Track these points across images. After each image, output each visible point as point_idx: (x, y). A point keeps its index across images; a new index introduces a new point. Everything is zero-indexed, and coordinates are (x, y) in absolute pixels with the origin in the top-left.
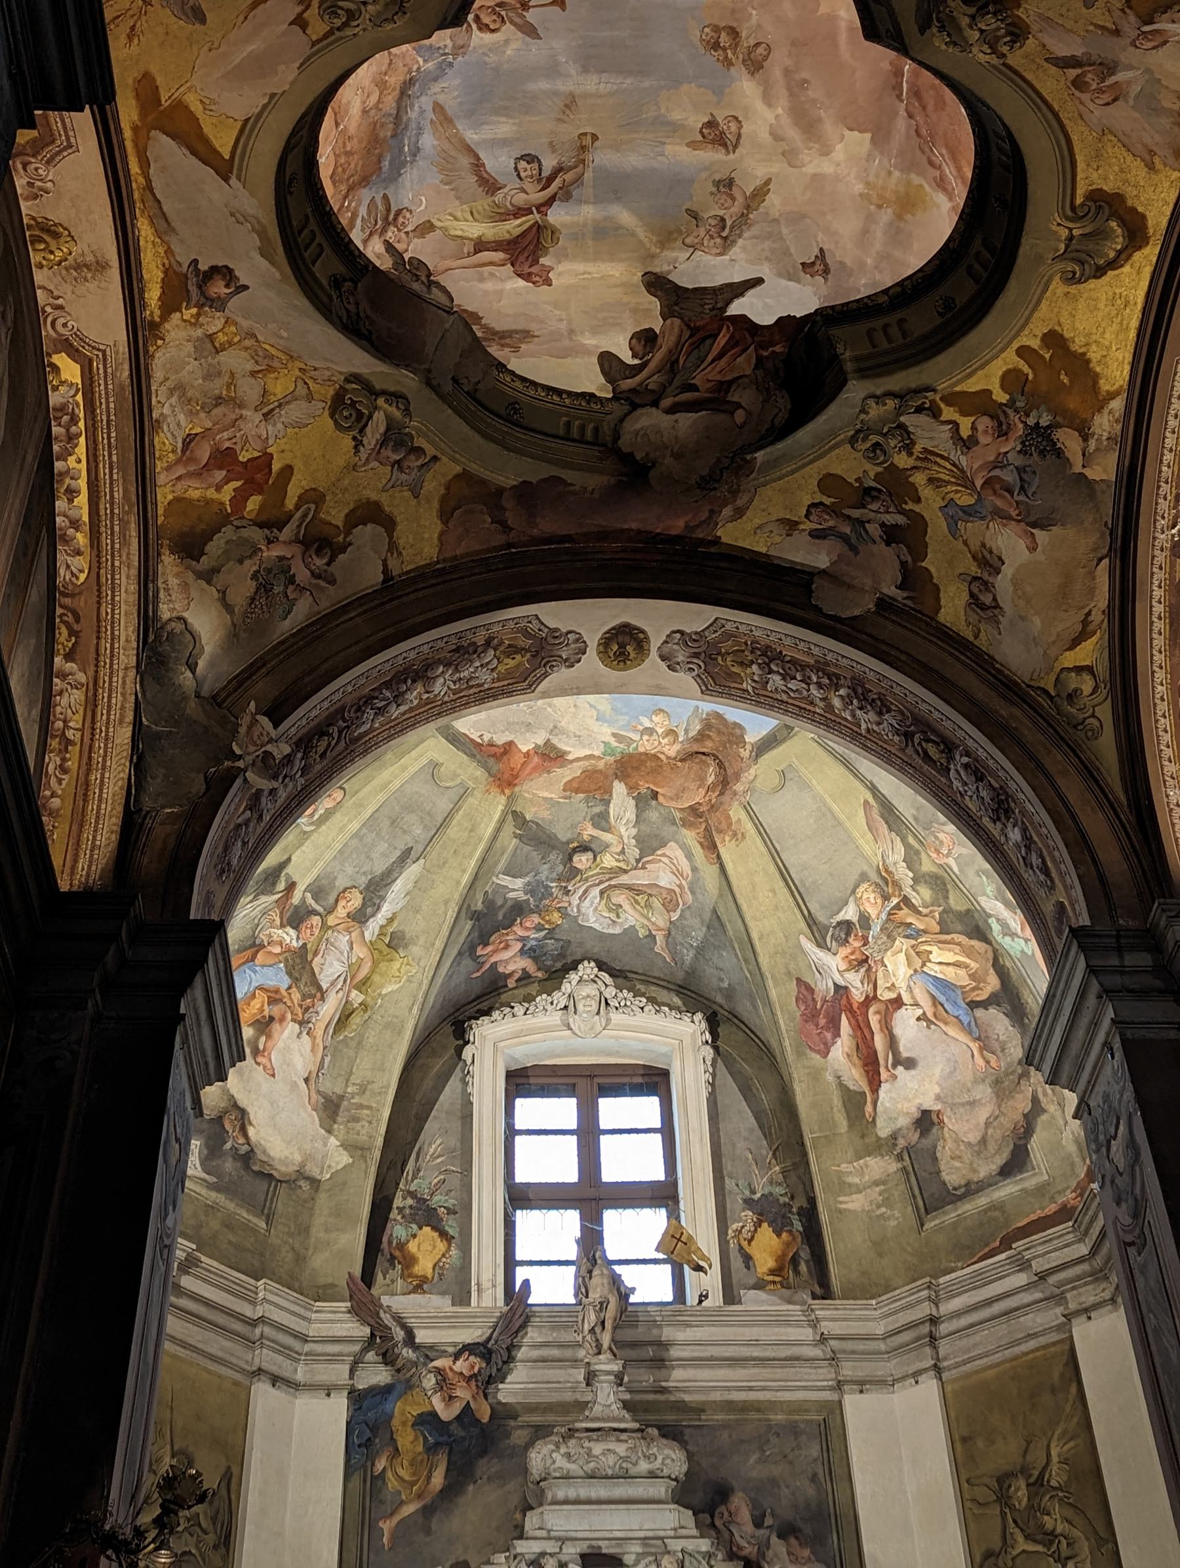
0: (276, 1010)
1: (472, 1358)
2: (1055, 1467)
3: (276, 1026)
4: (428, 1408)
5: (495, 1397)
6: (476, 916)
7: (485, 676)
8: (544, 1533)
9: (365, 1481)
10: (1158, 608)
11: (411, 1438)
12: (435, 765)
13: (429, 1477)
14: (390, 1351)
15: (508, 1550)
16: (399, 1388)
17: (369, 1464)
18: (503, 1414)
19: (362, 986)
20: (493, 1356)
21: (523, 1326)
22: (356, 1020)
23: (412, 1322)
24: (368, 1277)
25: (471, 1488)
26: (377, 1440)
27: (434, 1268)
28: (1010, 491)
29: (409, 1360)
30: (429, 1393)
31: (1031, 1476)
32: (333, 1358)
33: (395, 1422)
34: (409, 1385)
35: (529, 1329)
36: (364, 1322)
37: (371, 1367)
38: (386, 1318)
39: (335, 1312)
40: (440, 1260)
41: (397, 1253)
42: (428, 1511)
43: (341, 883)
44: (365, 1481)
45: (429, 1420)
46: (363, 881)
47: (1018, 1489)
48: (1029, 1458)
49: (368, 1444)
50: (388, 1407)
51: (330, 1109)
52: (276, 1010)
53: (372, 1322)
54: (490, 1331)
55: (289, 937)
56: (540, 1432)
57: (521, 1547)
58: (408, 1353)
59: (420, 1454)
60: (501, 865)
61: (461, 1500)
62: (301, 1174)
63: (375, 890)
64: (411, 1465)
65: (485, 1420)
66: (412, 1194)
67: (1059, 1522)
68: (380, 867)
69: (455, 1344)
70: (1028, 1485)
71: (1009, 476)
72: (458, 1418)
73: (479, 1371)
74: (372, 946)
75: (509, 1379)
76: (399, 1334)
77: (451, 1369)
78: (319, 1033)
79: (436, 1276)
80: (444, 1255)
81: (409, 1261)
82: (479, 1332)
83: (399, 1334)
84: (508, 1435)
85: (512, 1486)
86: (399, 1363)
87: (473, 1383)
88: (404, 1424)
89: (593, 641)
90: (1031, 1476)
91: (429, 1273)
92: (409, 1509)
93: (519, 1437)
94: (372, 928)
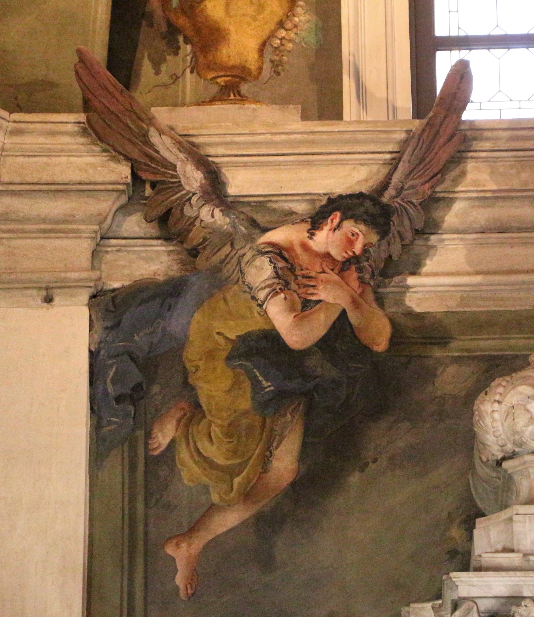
1: (349, 226)
4: (255, 325)
5: (400, 302)
8: (514, 559)
9: (133, 467)
11: (226, 383)
13: (266, 459)
14: (176, 212)
15: (439, 596)
16: (197, 283)
17: (140, 433)
18: (420, 335)
20: (391, 219)
21: (457, 159)
23: (216, 152)
24: (122, 61)
25: (355, 479)
26: (156, 389)
27: (261, 50)
29: (215, 231)
30: (261, 295)
32: (55, 228)
33: (192, 354)
34: (219, 281)
35: (470, 165)
36: (117, 153)
37: (138, 247)
38: (165, 147)
39: (53, 134)
40: (272, 35)
41: (182, 21)
44: (133, 467)
45: (263, 347)
49: (135, 396)
50: (175, 323)
53: (135, 154)
54: (384, 171)
56: (498, 367)
57: (466, 584)
58: (212, 217)
59: (245, 413)
61: (338, 502)
64: (229, 434)
65: (381, 344)
69: (310, 197)
72: (325, 344)
73: (365, 250)
75: (429, 265)
76: (193, 178)
77: (305, 247)
79: (267, 66)
80: (281, 24)
81: (208, 38)
82: (362, 173)
83: (193, 178)
84: (429, 375)
85: (442, 473)
86: (196, 236)
87: (353, 275)
88: (210, 355)
91: (251, 59)
92: (229, 520)
93: (450, 379)
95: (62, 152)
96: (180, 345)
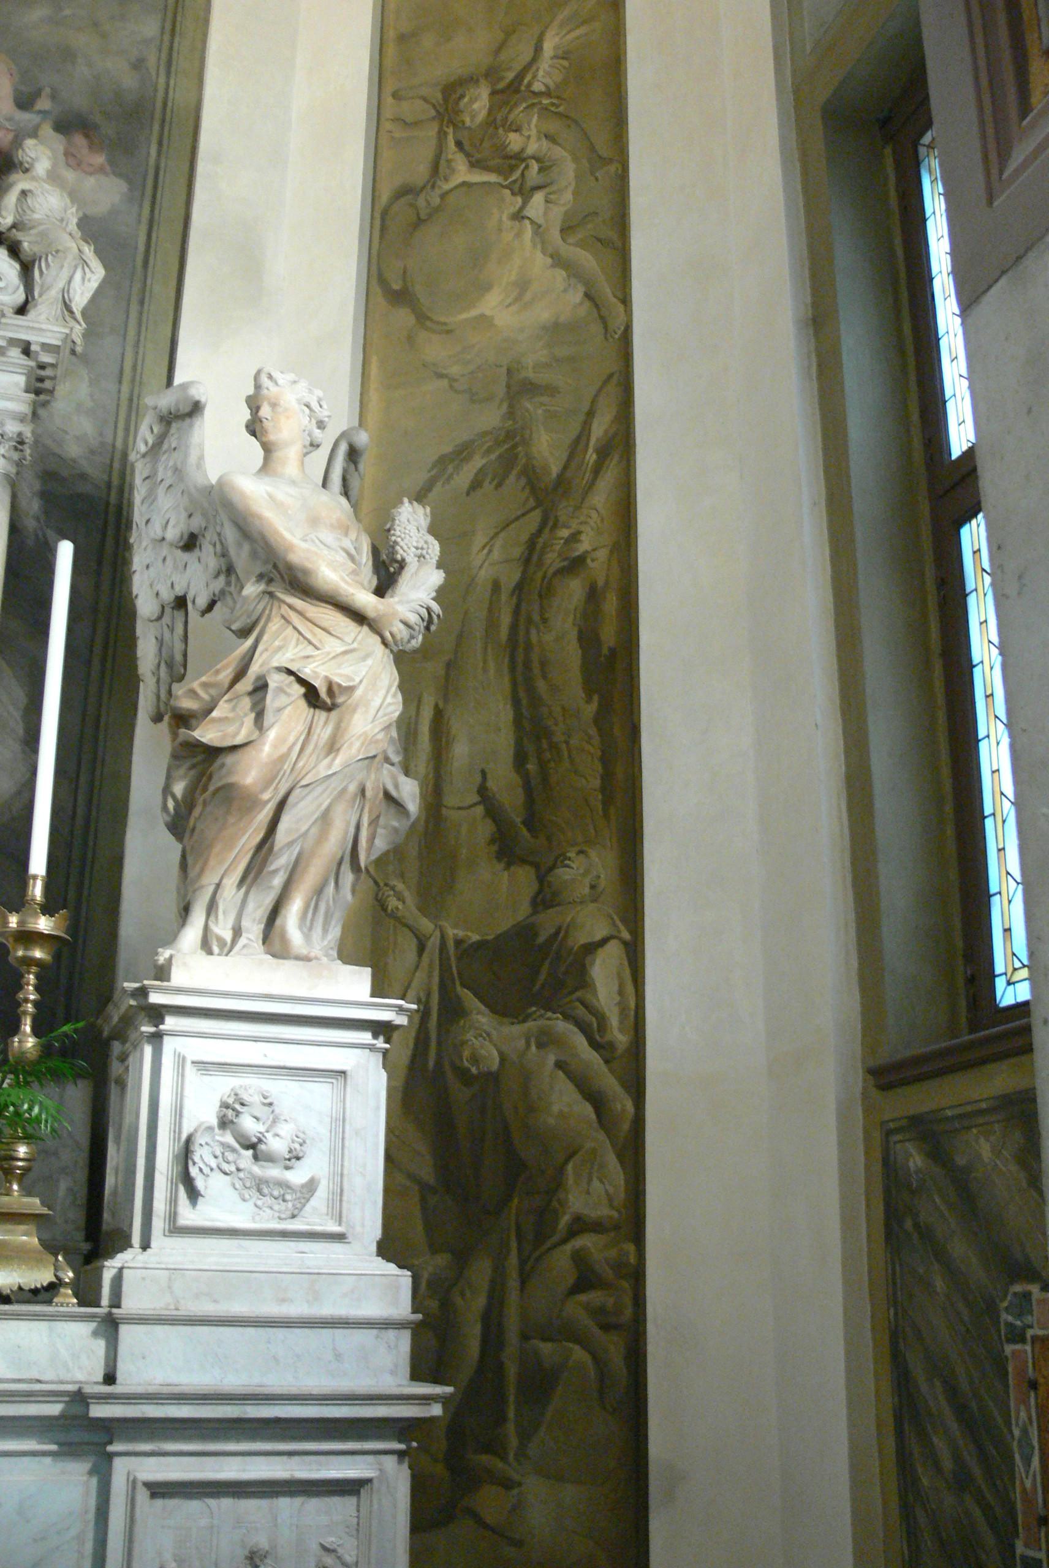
2: (545, 65)
31: (502, 78)
47: (473, 101)
48: (504, 56)
67: (533, 139)
70: (493, 93)
90: (502, 78)
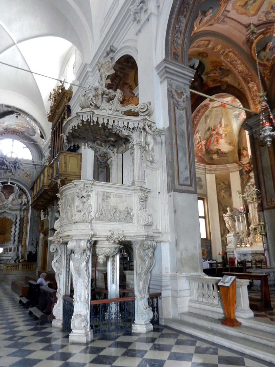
0: (218, 139)
3: (219, 140)
6: (234, 118)
7: (203, 111)
10: (241, 80)
12: (216, 110)
19: (226, 131)
22: (227, 134)
28: (222, 75)
42: (248, 180)
43: (216, 125)
45: (246, 171)
46: (219, 123)
51: (230, 144)
52: (218, 139)
55: (215, 132)
58: (243, 165)
60: (232, 112)
62: (229, 151)
63: (220, 123)
66: (243, 147)
68: (219, 121)
71: (221, 73)
74: (224, 127)
78: (224, 138)
89: (209, 102)
92: (246, 180)
94: (223, 126)
95: (235, 165)
96: (243, 172)
